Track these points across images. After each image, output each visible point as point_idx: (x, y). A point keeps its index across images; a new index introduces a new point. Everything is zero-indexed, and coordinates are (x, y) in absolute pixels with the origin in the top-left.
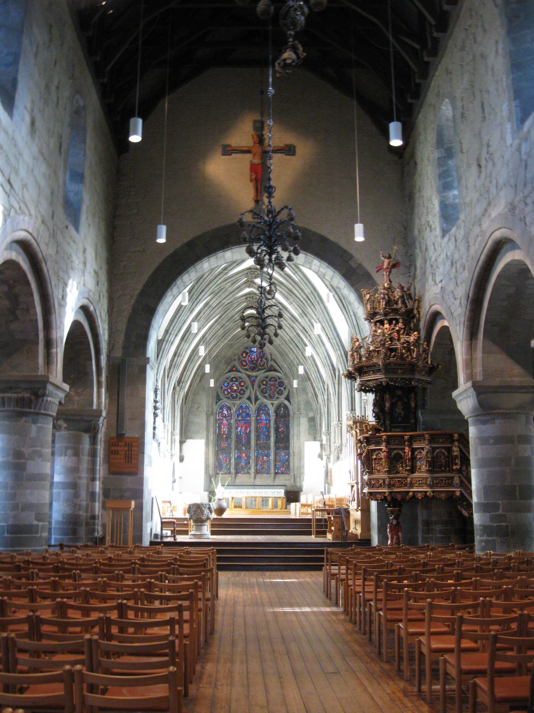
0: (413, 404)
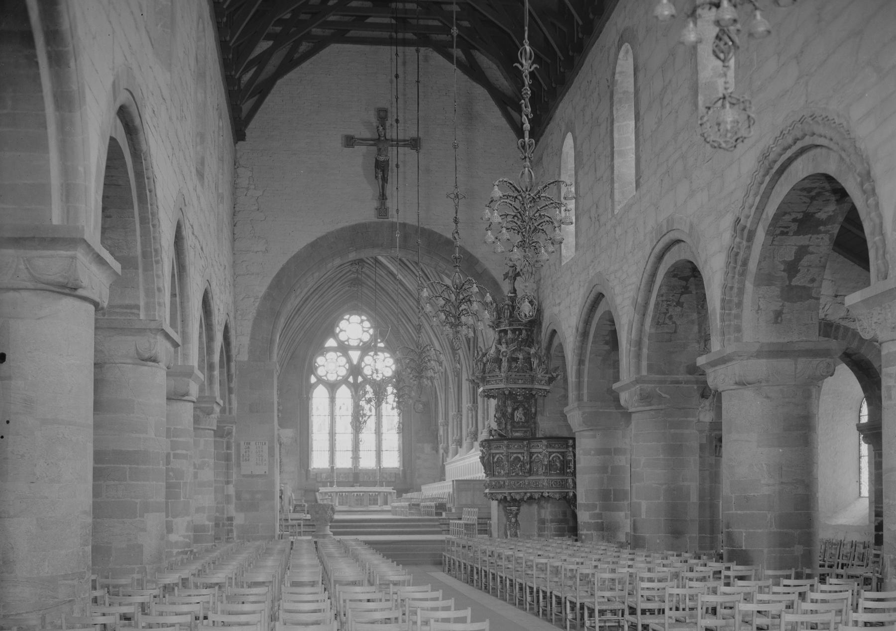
0: (533, 410)
